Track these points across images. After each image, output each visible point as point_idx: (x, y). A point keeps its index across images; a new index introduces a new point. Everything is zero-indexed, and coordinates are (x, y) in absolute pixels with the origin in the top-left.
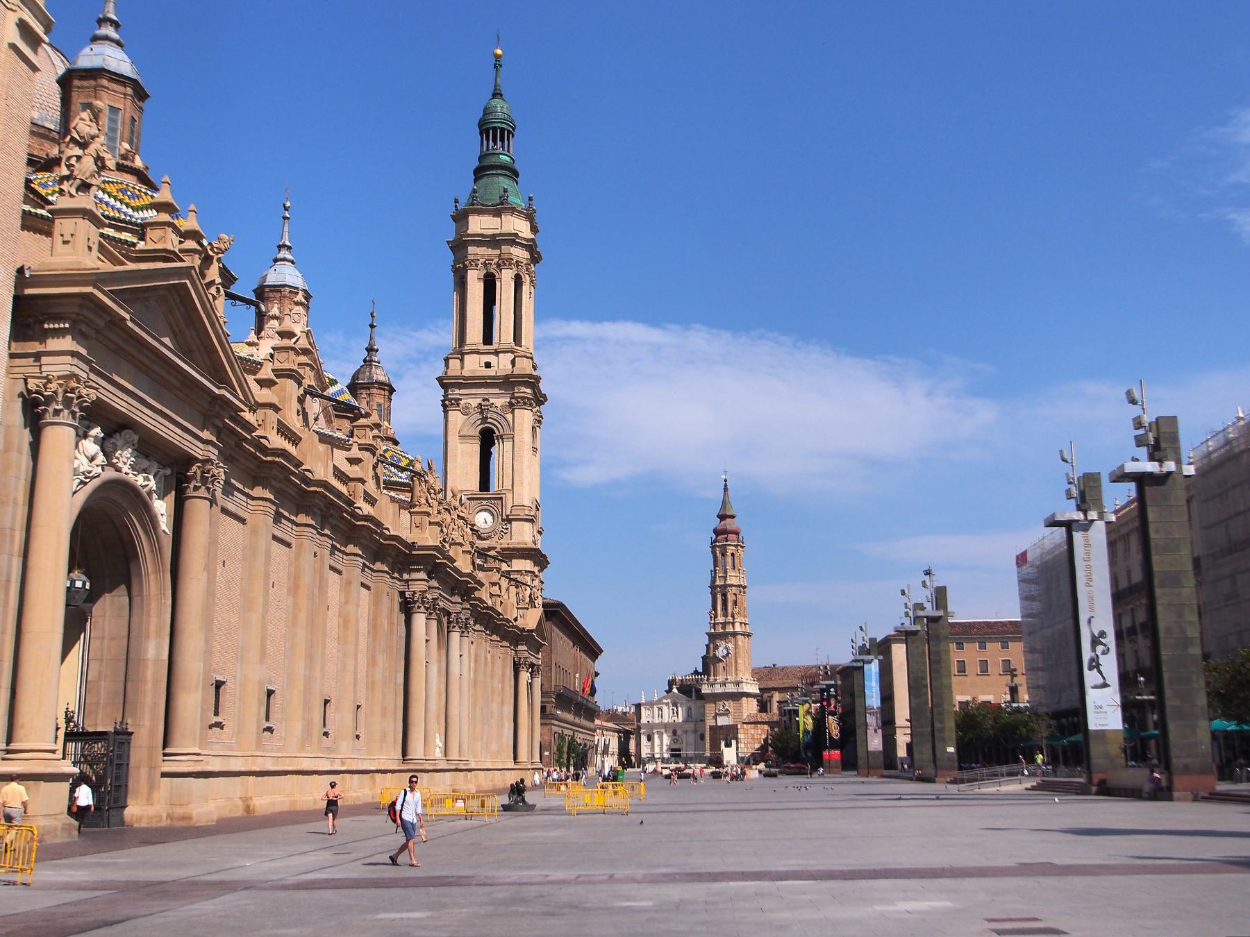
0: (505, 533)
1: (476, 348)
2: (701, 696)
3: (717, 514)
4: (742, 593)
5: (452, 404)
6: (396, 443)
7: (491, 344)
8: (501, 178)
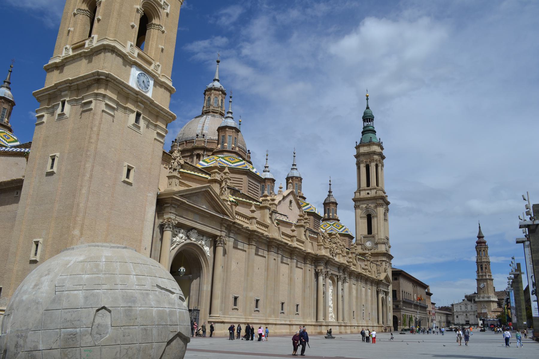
0: (376, 248)
3: (477, 236)
5: (357, 207)
6: (339, 220)
7: (369, 187)
8: (370, 134)
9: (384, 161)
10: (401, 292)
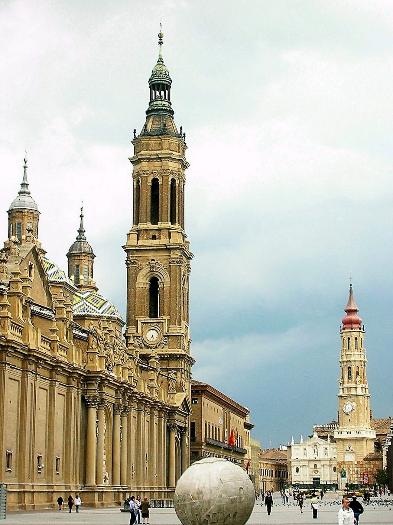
1: (147, 227)
2: (333, 440)
4: (363, 366)
6: (96, 289)
9: (187, 172)
10: (203, 427)
